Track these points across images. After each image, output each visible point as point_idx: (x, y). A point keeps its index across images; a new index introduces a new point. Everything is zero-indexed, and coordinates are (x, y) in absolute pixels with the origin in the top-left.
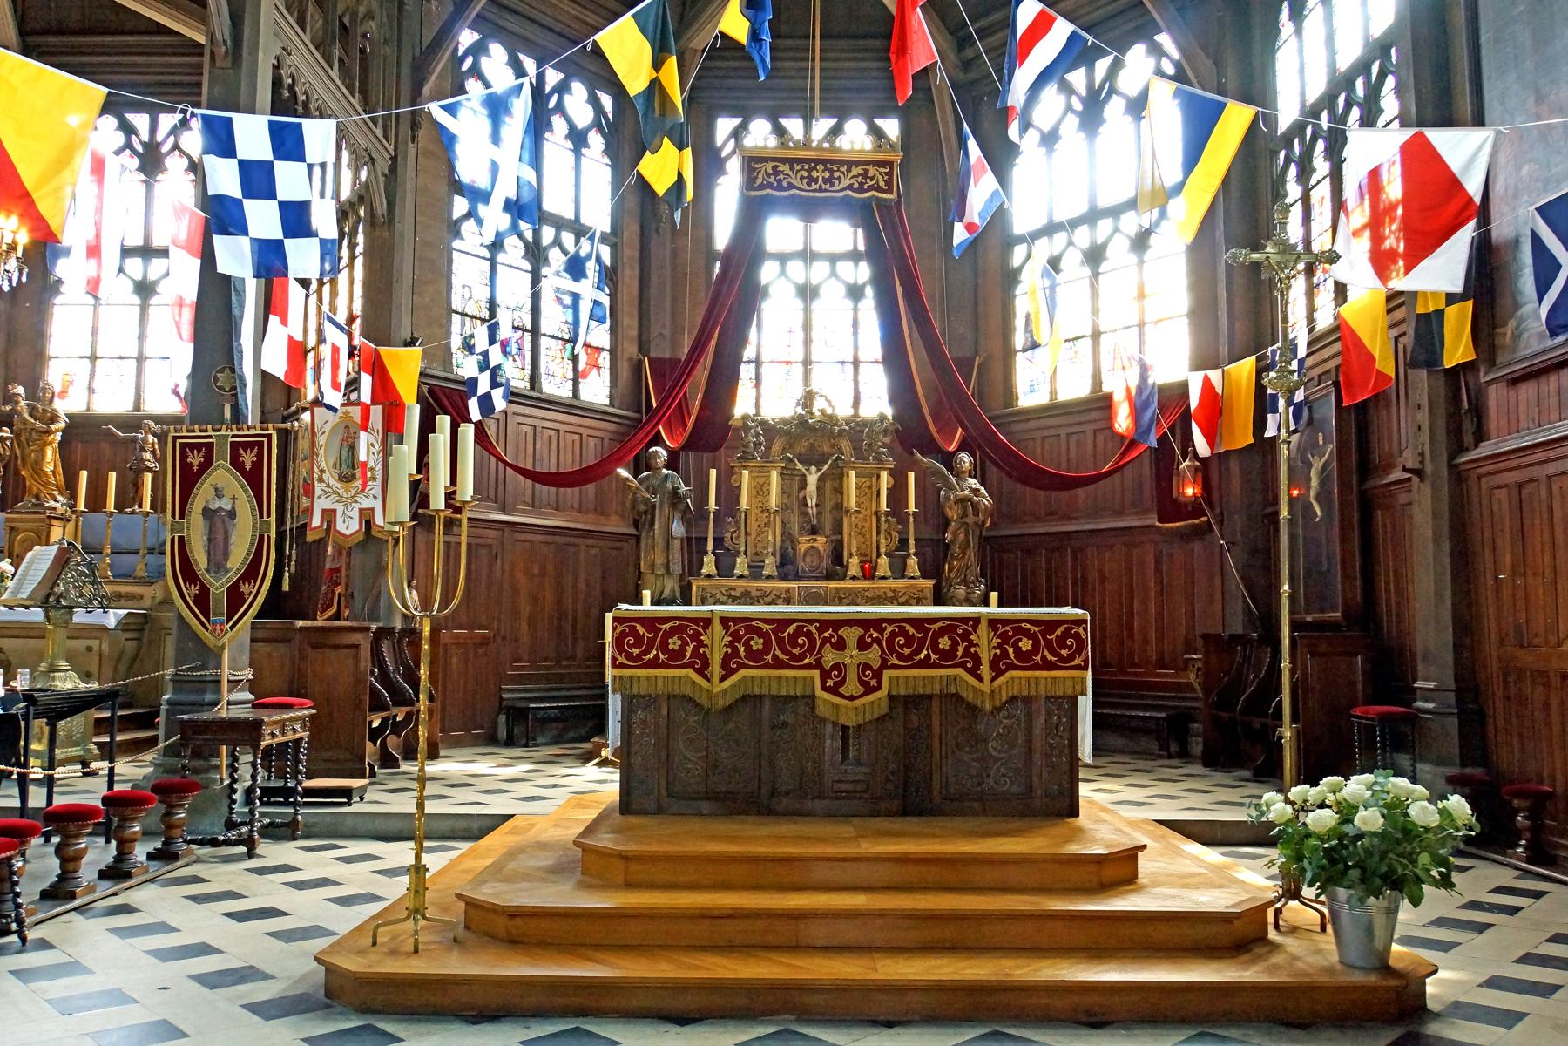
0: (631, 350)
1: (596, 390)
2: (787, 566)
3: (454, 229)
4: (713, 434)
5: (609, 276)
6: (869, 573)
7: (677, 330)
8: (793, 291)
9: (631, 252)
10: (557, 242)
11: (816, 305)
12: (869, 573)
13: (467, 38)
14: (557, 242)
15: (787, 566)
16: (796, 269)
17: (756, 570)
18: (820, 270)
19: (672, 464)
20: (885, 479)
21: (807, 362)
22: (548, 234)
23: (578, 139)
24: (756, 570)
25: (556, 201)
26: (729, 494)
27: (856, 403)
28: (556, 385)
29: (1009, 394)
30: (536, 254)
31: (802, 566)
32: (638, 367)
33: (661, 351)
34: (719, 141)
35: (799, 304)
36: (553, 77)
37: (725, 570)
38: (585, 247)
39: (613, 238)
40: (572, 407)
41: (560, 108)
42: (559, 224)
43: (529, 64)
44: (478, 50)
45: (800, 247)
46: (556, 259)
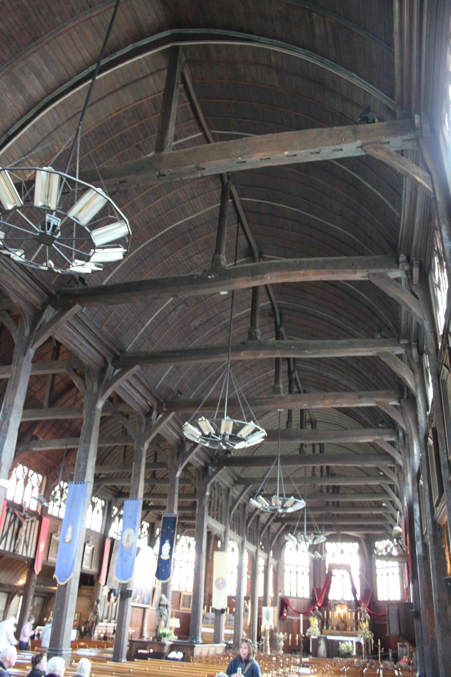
0: (312, 586)
2: (338, 628)
4: (326, 604)
5: (309, 574)
6: (352, 630)
7: (320, 582)
9: (312, 569)
12: (352, 630)
15: (338, 628)
17: (332, 628)
19: (320, 609)
20: (354, 614)
24: (332, 628)
26: (328, 615)
28: (300, 596)
29: (377, 597)
30: (297, 573)
31: (341, 628)
32: (313, 590)
33: (317, 587)
37: (327, 628)
40: (303, 598)
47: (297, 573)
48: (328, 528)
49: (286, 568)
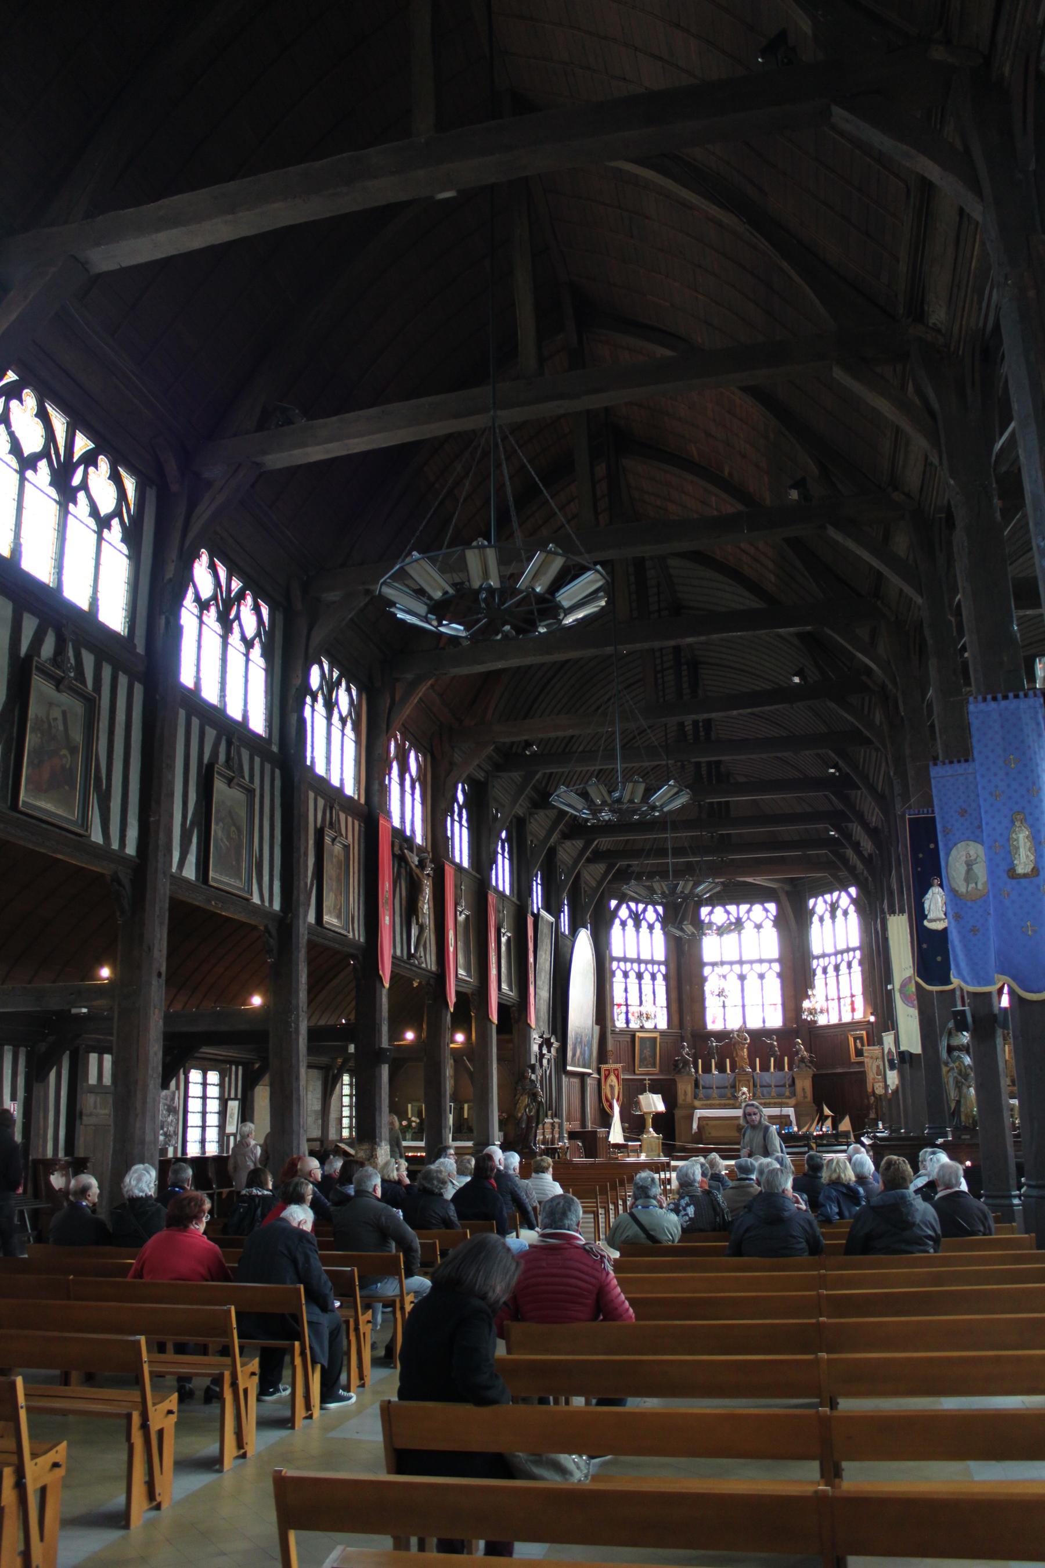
1: (662, 1024)
3: (613, 973)
5: (666, 978)
8: (736, 977)
9: (673, 966)
10: (646, 969)
11: (746, 982)
13: (613, 903)
14: (646, 969)
16: (737, 968)
18: (746, 968)
21: (743, 1006)
22: (643, 966)
23: (651, 927)
25: (645, 956)
27: (764, 1022)
30: (640, 976)
34: (703, 918)
35: (739, 982)
36: (641, 907)
38: (656, 967)
39: (666, 963)
41: (644, 918)
42: (646, 962)
43: (633, 905)
44: (618, 907)
45: (737, 958)
46: (647, 976)
47: (640, 976)
48: (714, 870)
49: (615, 965)
